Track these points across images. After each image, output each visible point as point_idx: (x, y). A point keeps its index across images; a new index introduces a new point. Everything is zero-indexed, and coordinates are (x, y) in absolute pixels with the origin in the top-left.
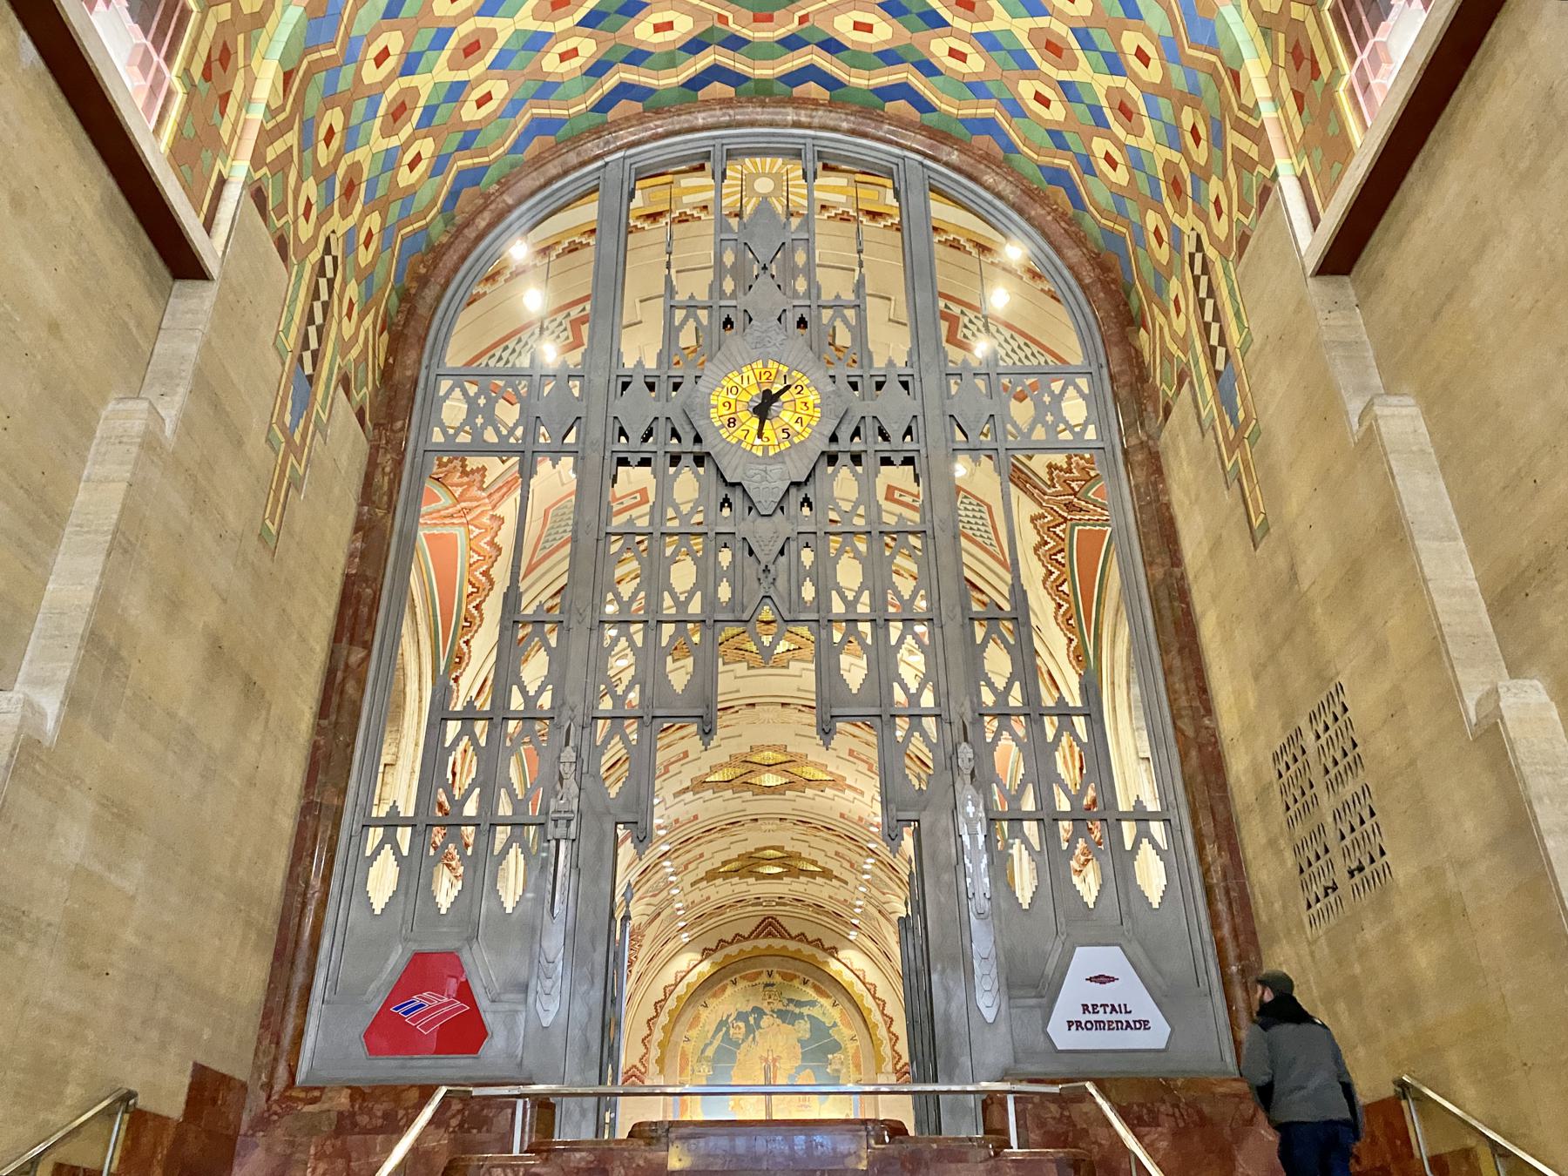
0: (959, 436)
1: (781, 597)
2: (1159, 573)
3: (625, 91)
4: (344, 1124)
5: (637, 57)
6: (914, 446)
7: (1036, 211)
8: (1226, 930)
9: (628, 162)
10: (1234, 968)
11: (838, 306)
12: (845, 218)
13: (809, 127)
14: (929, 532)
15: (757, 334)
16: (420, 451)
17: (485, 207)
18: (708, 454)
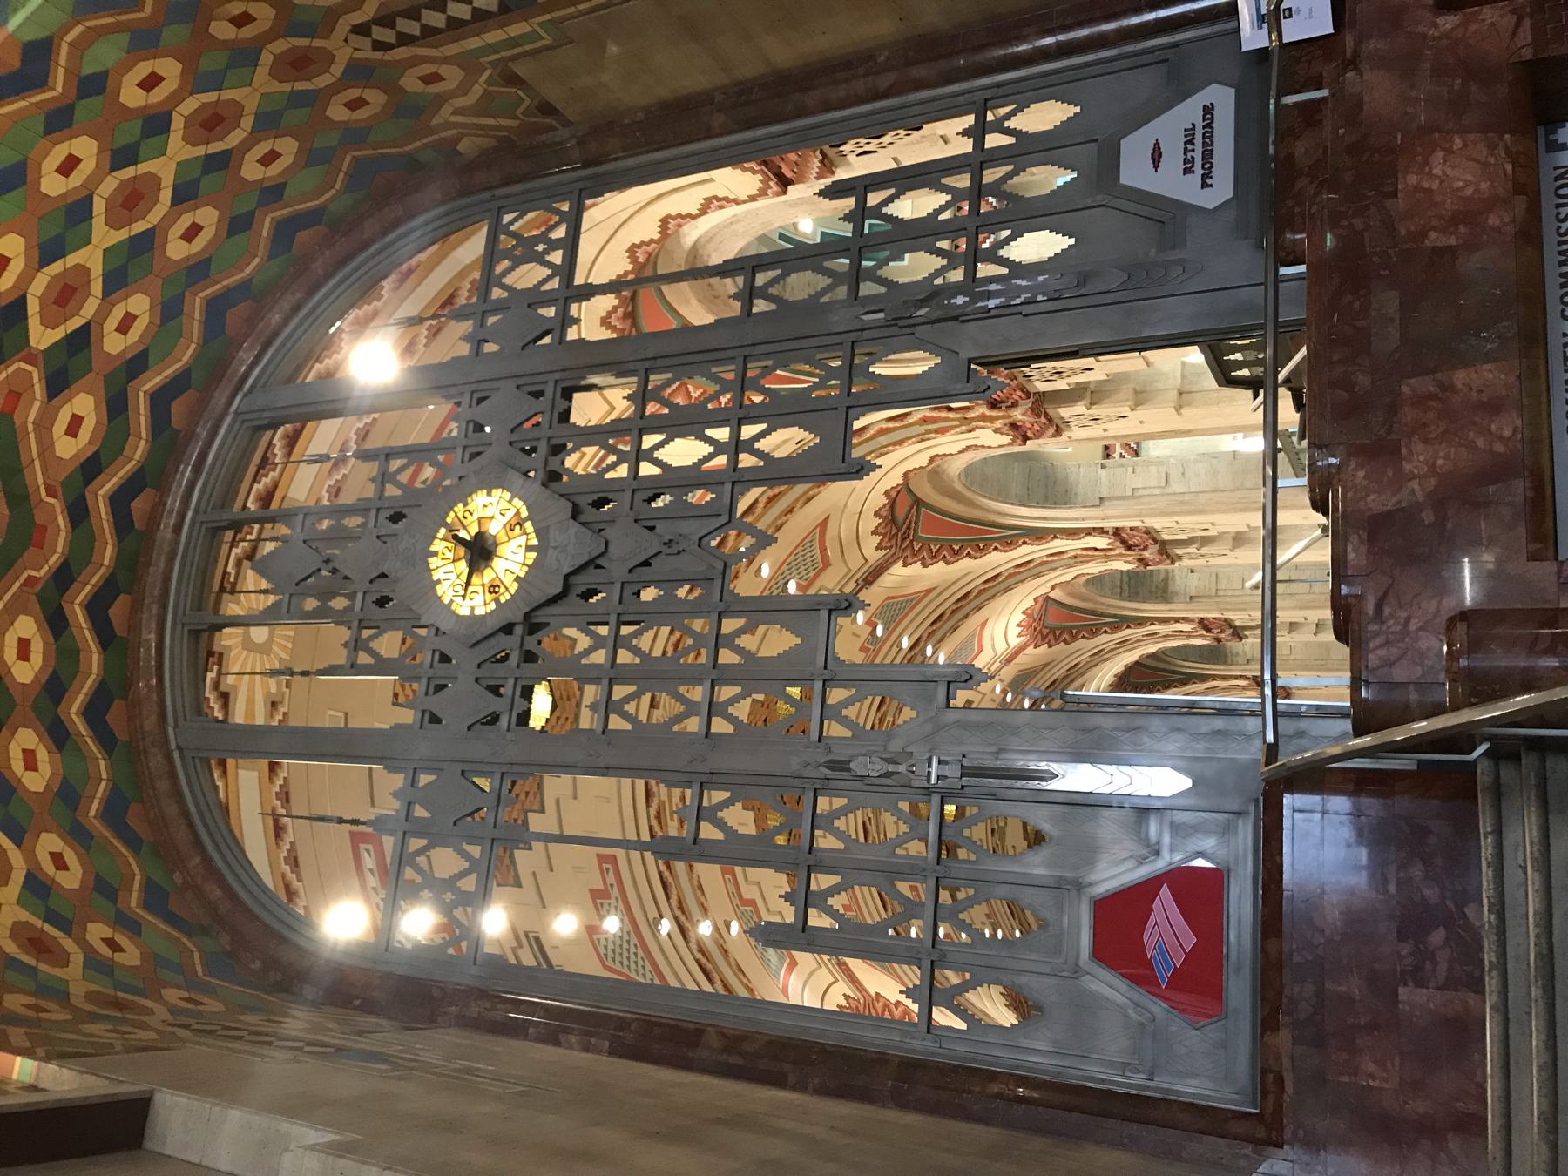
0: (547, 340)
2: (718, 120)
7: (318, 266)
11: (384, 478)
13: (182, 516)
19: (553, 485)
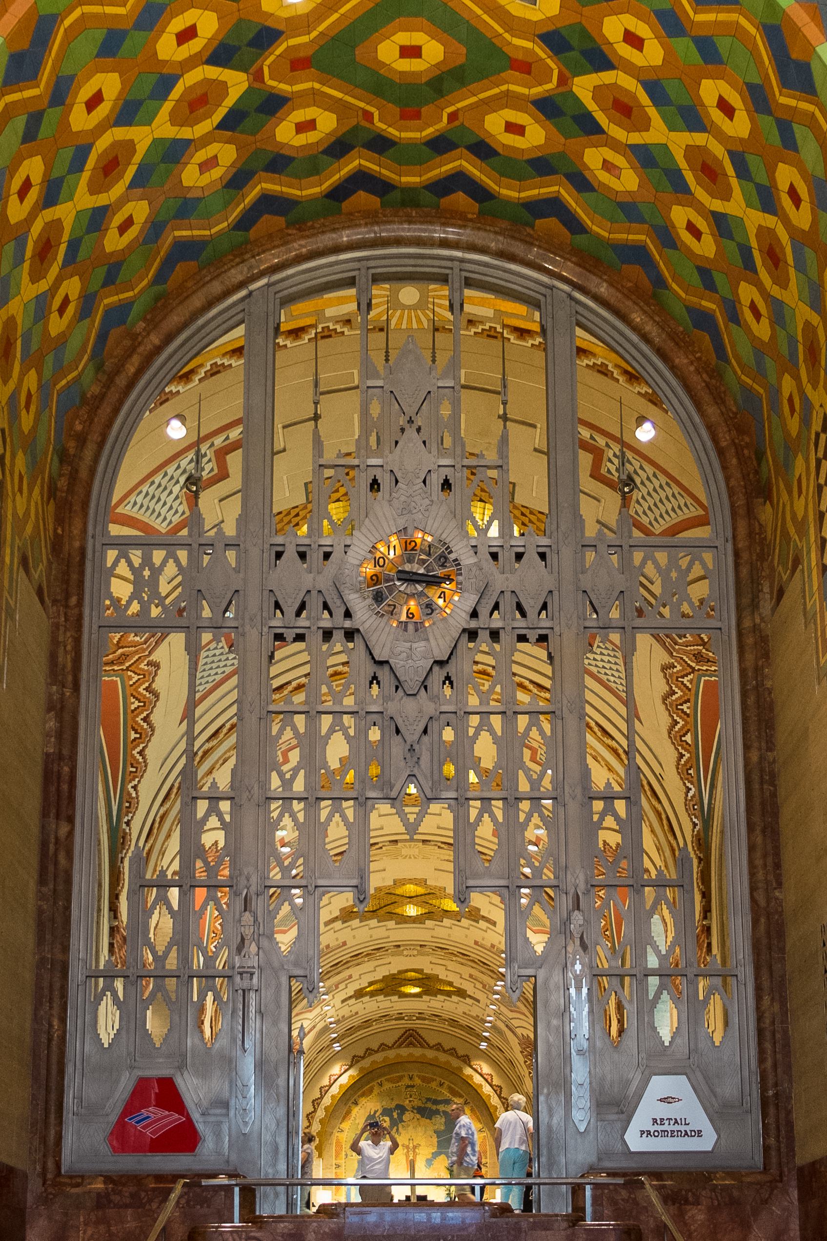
1: (425, 777)
3: (269, 204)
4: (102, 1201)
5: (279, 163)
6: (548, 624)
8: (769, 1063)
9: (272, 289)
10: (771, 1093)
12: (491, 334)
14: (558, 713)
15: (403, 498)
16: (95, 627)
17: (132, 350)
18: (358, 630)
19: (466, 636)
